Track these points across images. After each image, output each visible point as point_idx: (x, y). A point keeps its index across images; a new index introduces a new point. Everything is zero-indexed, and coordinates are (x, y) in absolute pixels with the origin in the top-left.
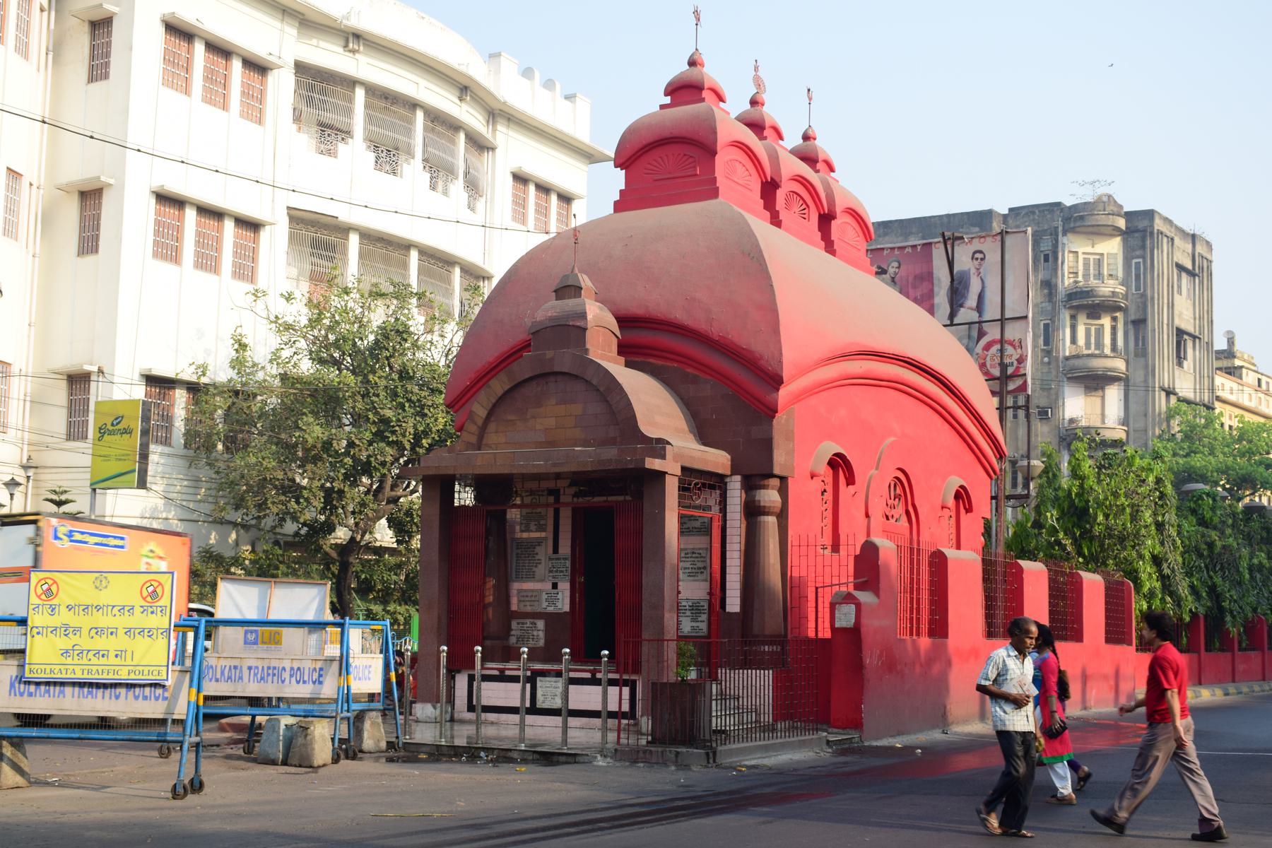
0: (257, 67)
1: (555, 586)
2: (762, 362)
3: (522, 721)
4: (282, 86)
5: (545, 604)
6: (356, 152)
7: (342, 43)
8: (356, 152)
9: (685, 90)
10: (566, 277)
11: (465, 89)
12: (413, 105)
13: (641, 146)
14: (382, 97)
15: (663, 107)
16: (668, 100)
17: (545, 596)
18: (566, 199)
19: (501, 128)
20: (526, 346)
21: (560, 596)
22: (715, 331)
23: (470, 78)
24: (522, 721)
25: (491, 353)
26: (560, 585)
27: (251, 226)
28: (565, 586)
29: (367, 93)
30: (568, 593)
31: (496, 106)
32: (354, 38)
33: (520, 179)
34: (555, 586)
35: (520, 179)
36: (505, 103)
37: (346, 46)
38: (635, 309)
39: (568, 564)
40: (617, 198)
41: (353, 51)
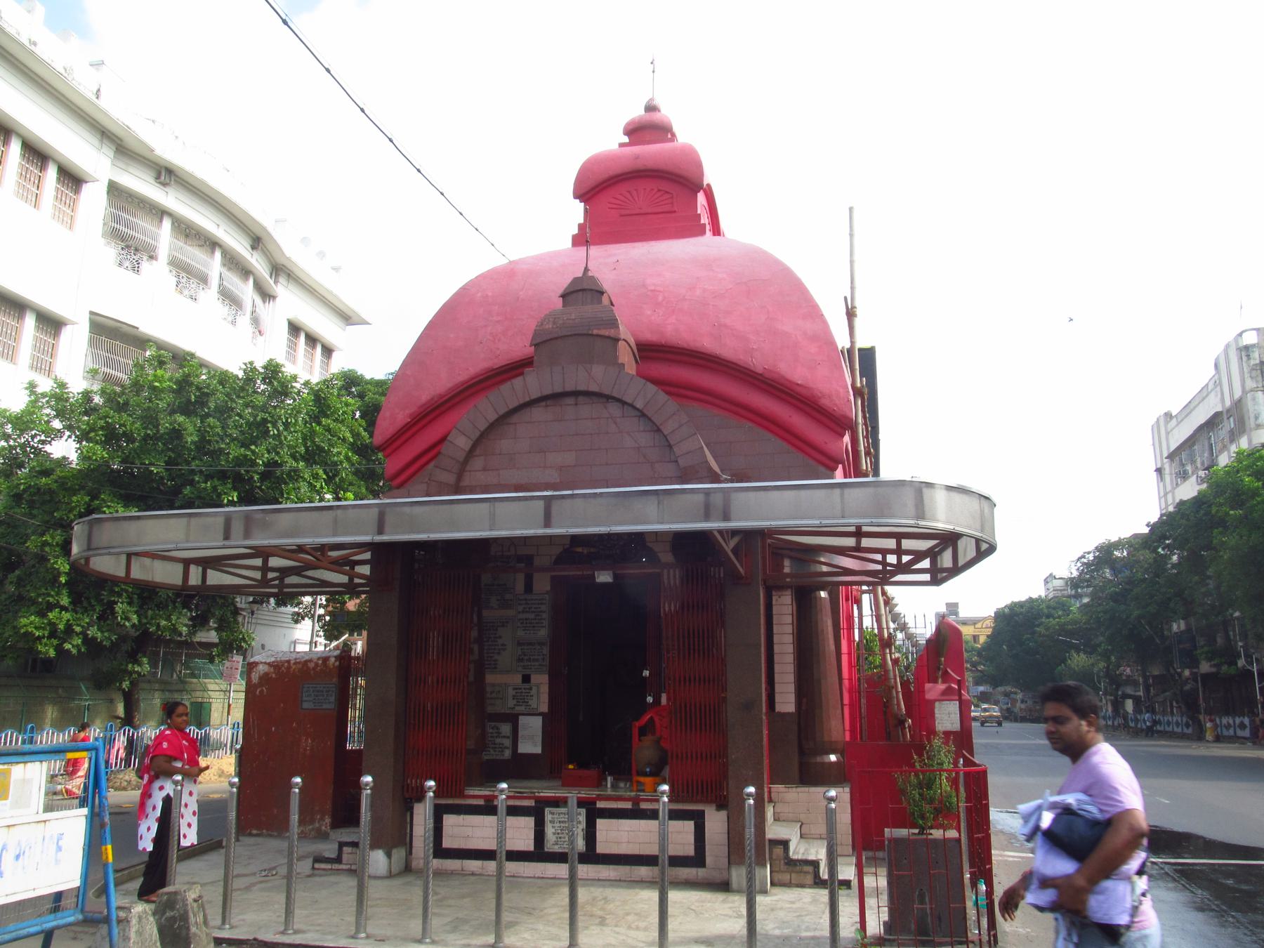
0: (72, 179)
1: (526, 679)
2: (825, 402)
3: (500, 869)
4: (94, 198)
5: (511, 703)
6: (157, 273)
7: (153, 174)
8: (157, 273)
9: (639, 131)
10: (576, 280)
11: (257, 241)
12: (212, 244)
13: (606, 176)
14: (186, 230)
15: (622, 145)
16: (626, 139)
17: (511, 692)
18: (328, 351)
19: (282, 280)
20: (516, 368)
21: (534, 691)
22: (758, 363)
23: (264, 229)
24: (500, 869)
25: (441, 382)
26: (535, 678)
27: (51, 324)
28: (541, 681)
29: (173, 224)
30: (545, 689)
31: (281, 260)
32: (166, 174)
33: (294, 329)
34: (526, 679)
35: (294, 329)
36: (289, 259)
37: (158, 177)
38: (649, 336)
39: (546, 650)
40: (576, 231)
41: (164, 184)
